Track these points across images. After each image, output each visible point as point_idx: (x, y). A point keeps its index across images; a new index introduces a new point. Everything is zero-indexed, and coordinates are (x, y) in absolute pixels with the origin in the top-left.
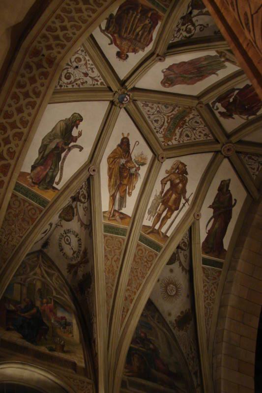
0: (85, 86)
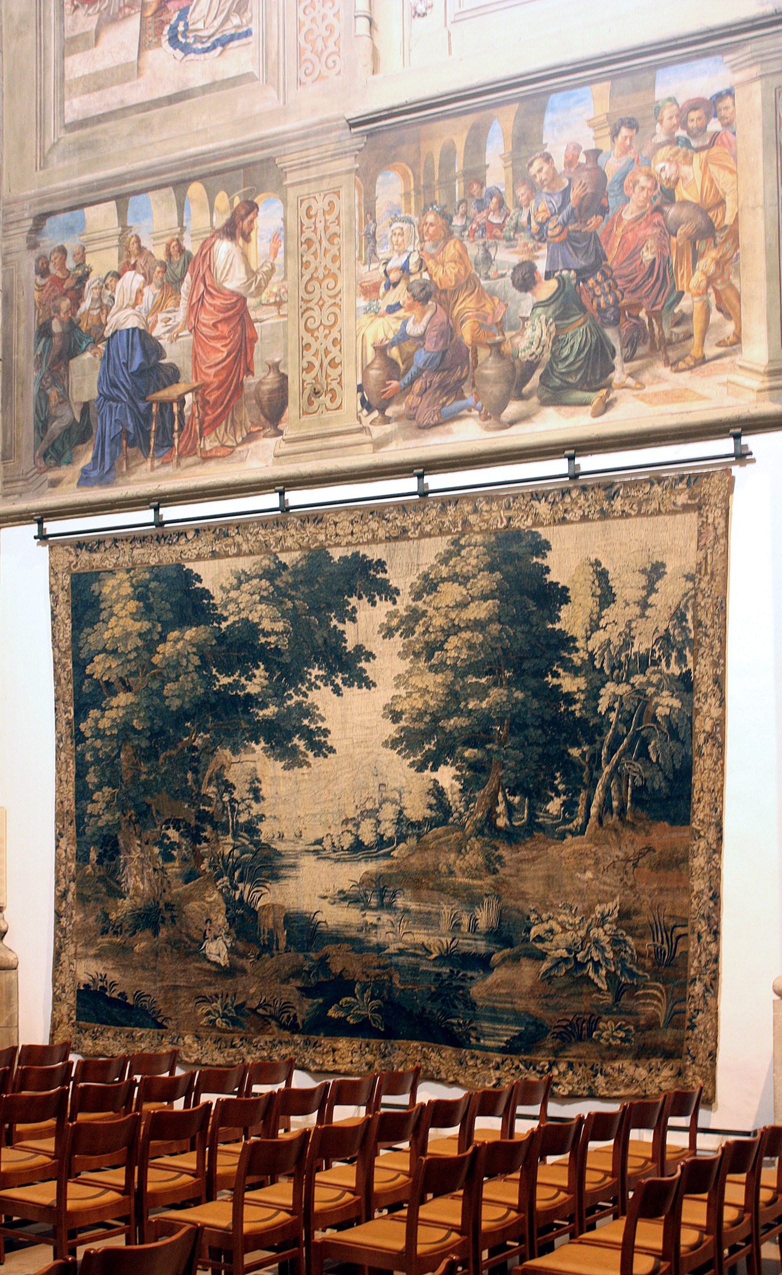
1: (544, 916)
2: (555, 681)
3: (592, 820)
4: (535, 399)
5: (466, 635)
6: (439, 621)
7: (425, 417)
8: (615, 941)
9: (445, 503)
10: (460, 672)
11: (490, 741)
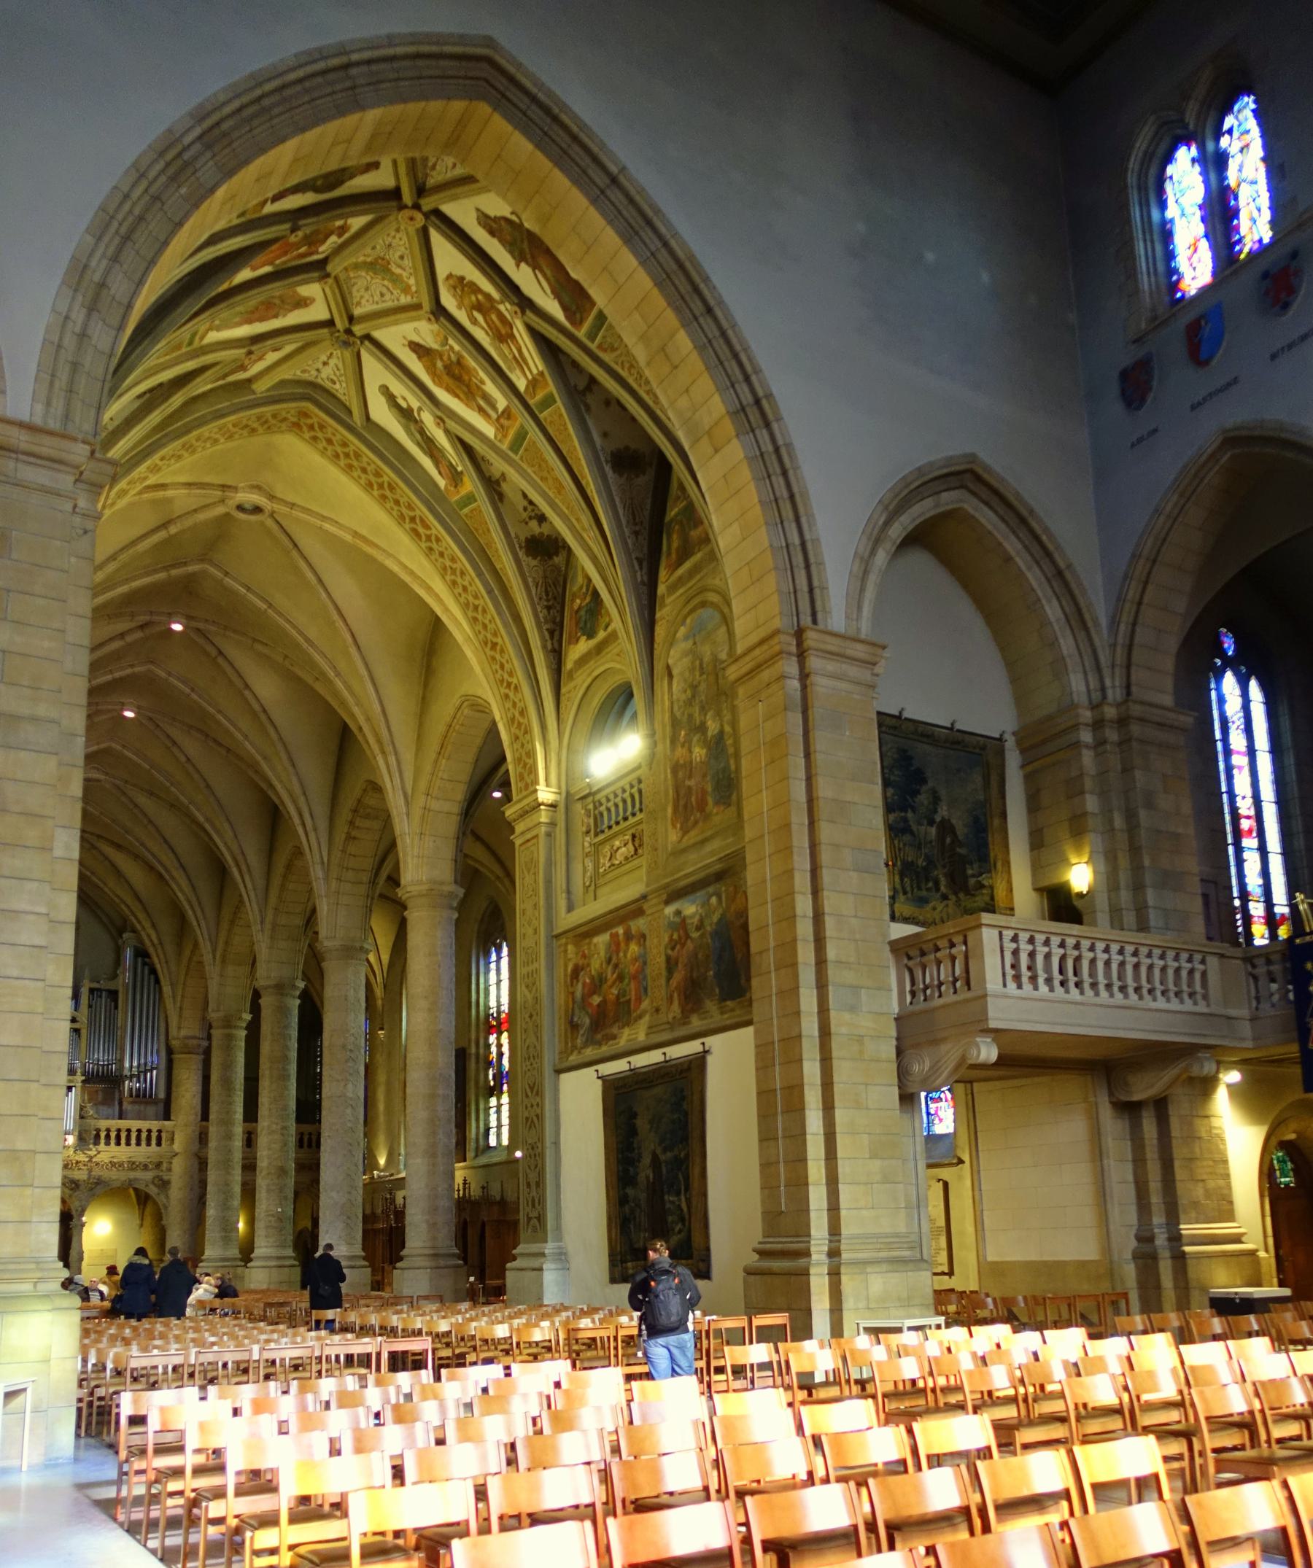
0: (341, 366)
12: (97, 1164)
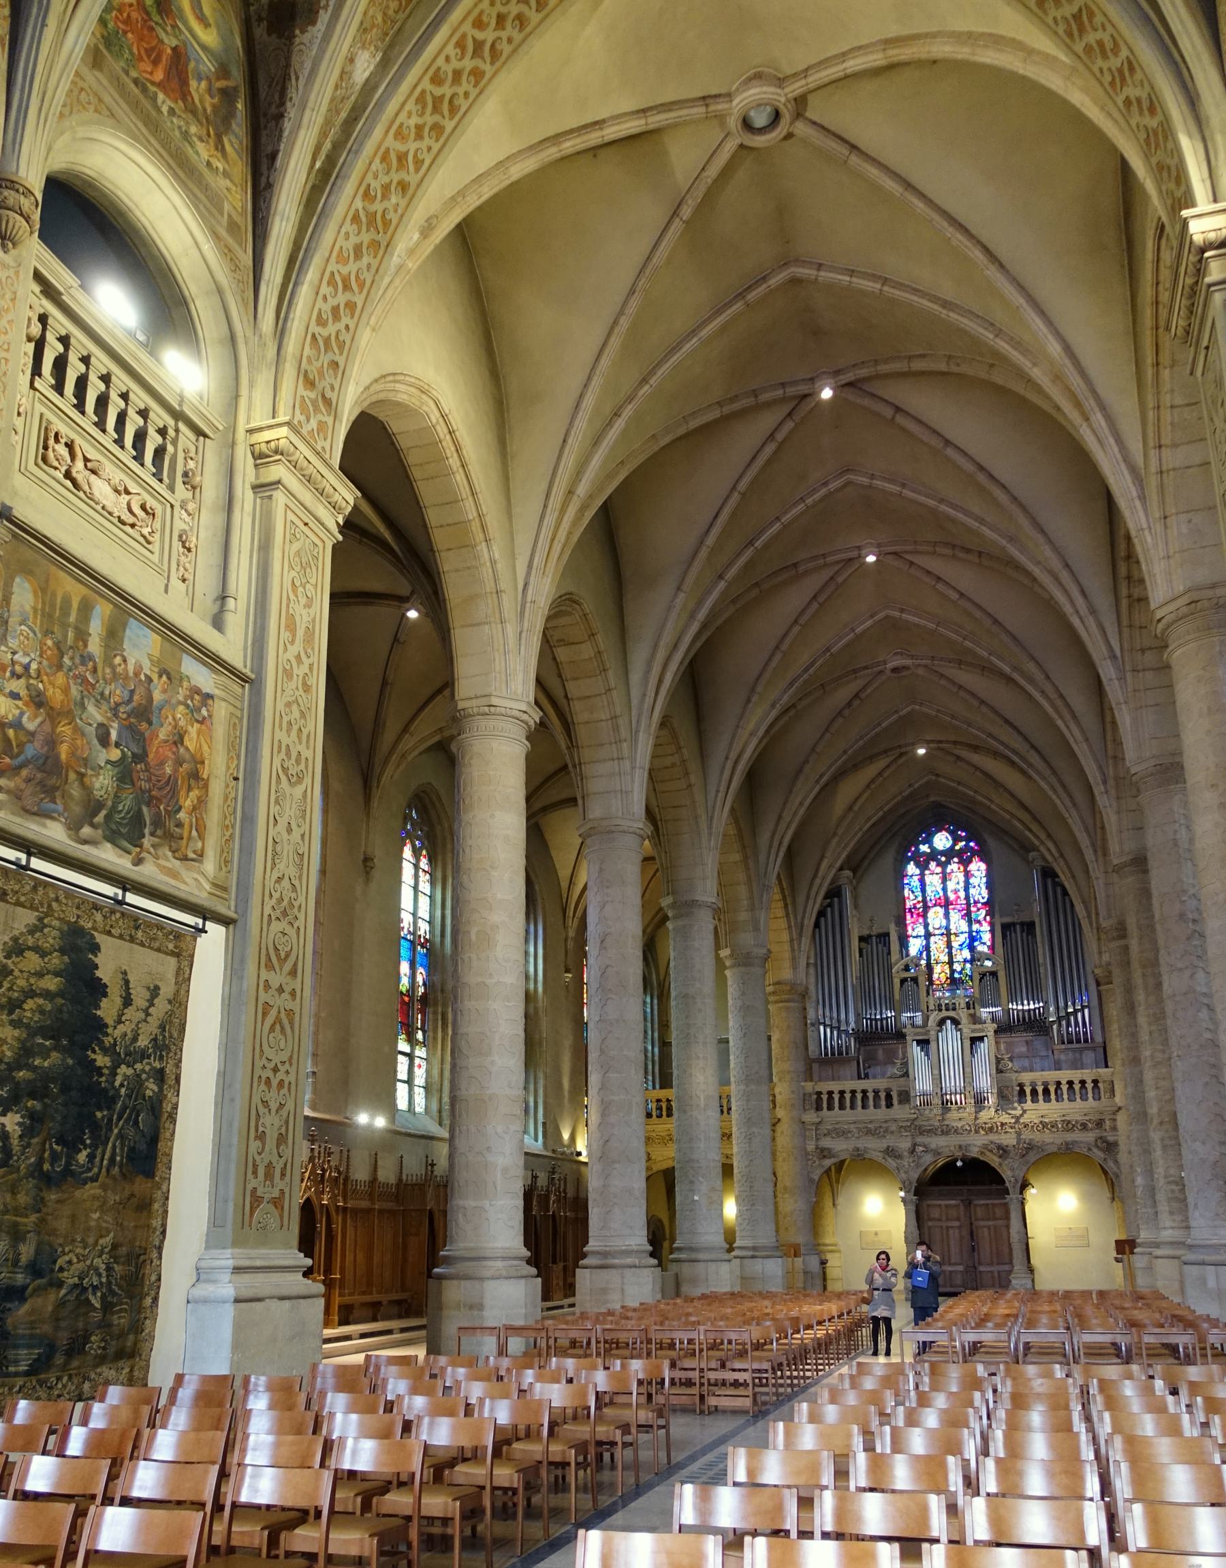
1: (67, 1249)
2: (93, 1056)
3: (104, 1170)
4: (100, 831)
5: (41, 1001)
6: (21, 983)
7: (29, 802)
8: (109, 1269)
9: (38, 884)
10: (33, 1031)
11: (47, 1096)
12: (1026, 1126)
